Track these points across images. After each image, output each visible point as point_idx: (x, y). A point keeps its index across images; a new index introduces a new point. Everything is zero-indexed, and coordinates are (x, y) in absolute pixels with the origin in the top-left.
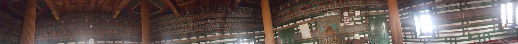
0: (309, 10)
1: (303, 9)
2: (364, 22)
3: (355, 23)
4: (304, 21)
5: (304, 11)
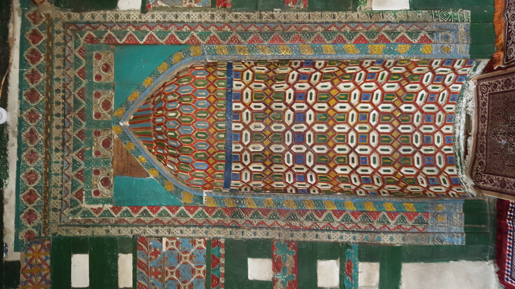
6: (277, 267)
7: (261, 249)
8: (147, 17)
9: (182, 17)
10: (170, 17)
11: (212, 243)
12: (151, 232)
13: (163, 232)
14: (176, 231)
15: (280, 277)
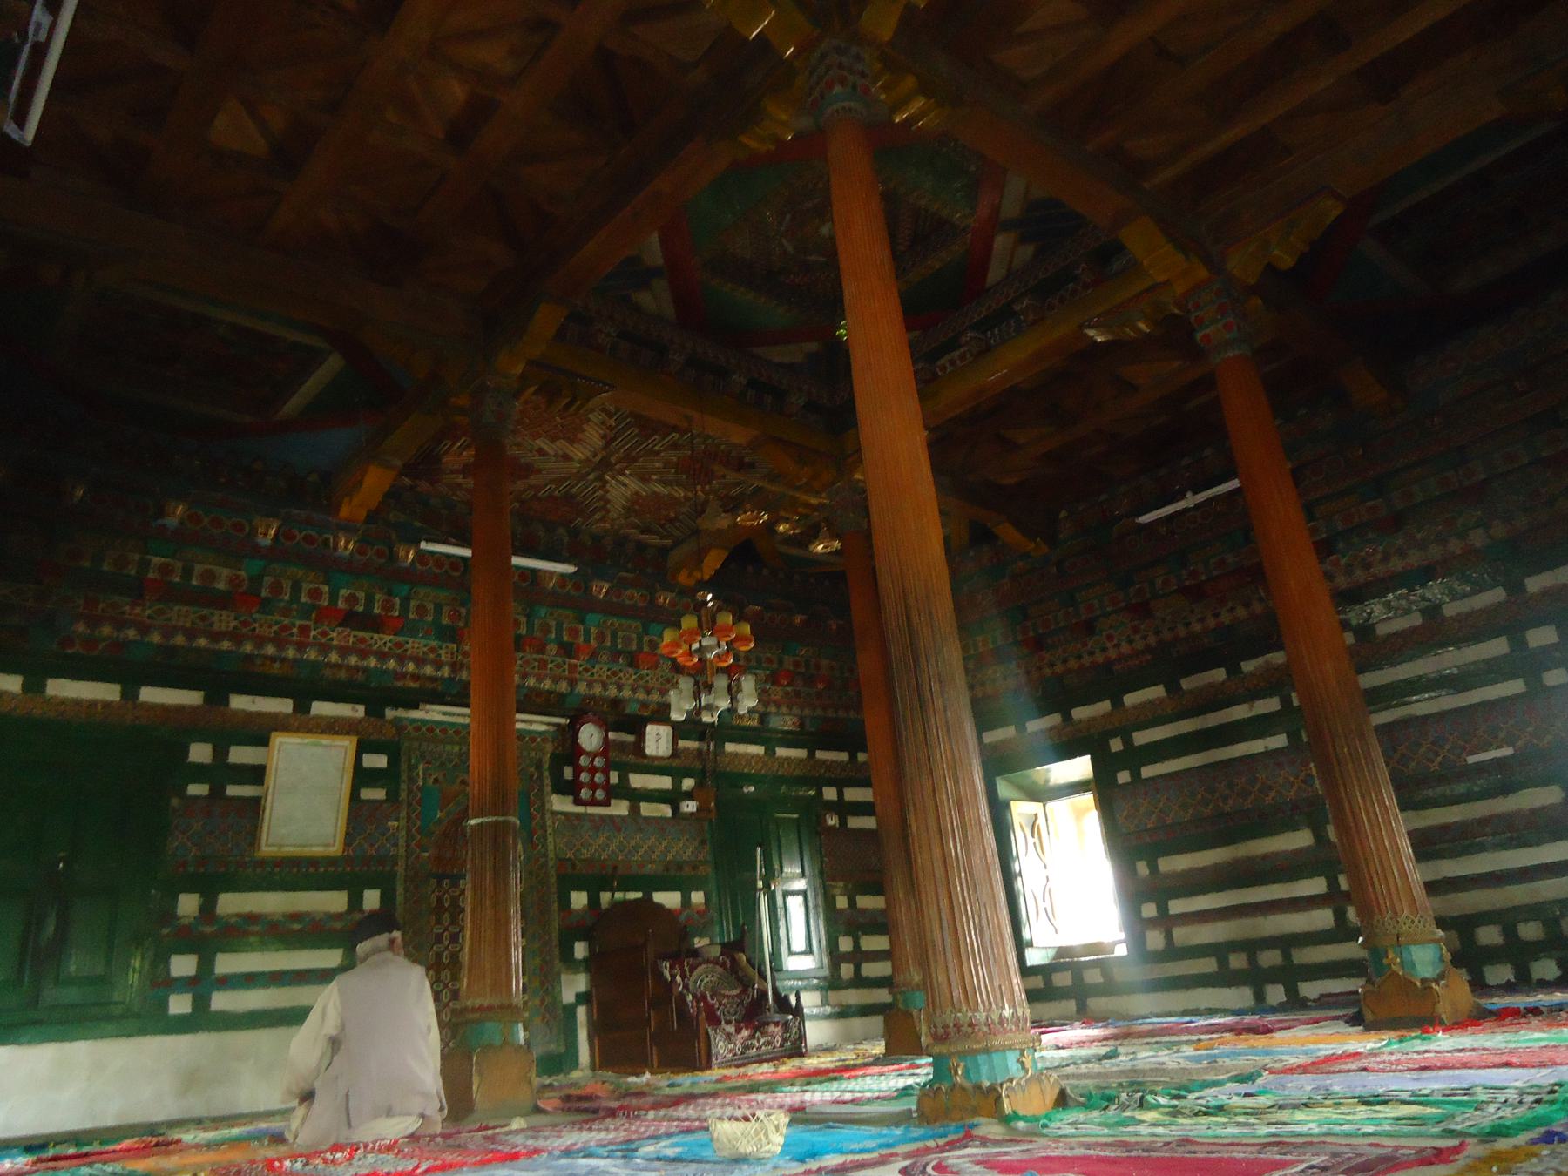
0: (384, 640)
1: (350, 619)
2: (690, 807)
3: (634, 810)
4: (302, 707)
8: (548, 816)
9: (550, 839)
11: (394, 860)
12: (403, 814)
13: (403, 823)
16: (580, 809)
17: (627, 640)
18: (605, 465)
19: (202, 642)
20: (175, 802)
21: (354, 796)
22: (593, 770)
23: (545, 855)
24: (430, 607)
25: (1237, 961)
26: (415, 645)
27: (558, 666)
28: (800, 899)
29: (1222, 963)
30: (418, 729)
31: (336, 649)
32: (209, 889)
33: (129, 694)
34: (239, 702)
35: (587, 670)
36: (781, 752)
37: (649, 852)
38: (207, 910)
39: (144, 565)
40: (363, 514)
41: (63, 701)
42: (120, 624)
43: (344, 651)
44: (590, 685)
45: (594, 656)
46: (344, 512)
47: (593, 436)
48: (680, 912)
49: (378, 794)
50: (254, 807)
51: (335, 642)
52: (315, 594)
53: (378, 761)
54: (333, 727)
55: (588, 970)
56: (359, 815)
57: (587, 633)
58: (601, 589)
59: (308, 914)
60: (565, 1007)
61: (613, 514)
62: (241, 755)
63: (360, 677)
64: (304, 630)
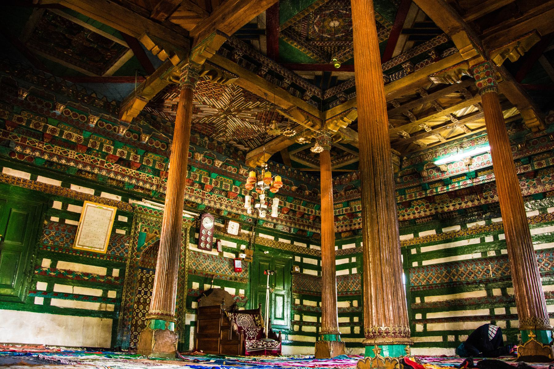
0: (132, 171)
1: (120, 161)
4: (98, 194)
5: (115, 167)
6: (116, 278)
7: (122, 273)
8: (187, 251)
9: (187, 260)
10: (187, 257)
12: (131, 241)
13: (131, 245)
14: (130, 249)
15: (113, 279)
16: (200, 251)
17: (226, 186)
18: (228, 112)
19: (64, 162)
20: (46, 222)
21: (114, 230)
22: (207, 236)
23: (184, 266)
24: (152, 161)
25: (451, 338)
26: (144, 175)
27: (198, 193)
28: (281, 298)
29: (445, 338)
30: (140, 209)
31: (113, 171)
32: (55, 257)
33: (34, 178)
34: (74, 188)
35: (209, 196)
36: (281, 240)
37: (224, 270)
38: (53, 266)
39: (46, 127)
40: (130, 120)
41: (8, 177)
42: (34, 150)
43: (116, 173)
44: (210, 202)
45: (212, 191)
46: (124, 118)
47: (226, 98)
48: (234, 296)
49: (123, 232)
50: (74, 229)
51: (113, 170)
52: (108, 149)
53: (125, 219)
54: (108, 203)
55: (196, 313)
56: (114, 239)
57: (211, 180)
58: (218, 163)
59: (91, 274)
60: (186, 326)
61: (228, 135)
62: (72, 208)
63: (121, 185)
64: (102, 163)
